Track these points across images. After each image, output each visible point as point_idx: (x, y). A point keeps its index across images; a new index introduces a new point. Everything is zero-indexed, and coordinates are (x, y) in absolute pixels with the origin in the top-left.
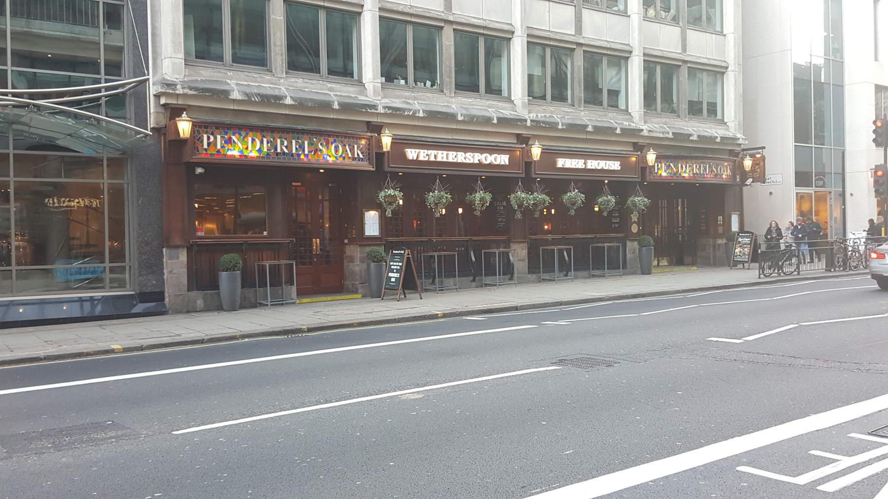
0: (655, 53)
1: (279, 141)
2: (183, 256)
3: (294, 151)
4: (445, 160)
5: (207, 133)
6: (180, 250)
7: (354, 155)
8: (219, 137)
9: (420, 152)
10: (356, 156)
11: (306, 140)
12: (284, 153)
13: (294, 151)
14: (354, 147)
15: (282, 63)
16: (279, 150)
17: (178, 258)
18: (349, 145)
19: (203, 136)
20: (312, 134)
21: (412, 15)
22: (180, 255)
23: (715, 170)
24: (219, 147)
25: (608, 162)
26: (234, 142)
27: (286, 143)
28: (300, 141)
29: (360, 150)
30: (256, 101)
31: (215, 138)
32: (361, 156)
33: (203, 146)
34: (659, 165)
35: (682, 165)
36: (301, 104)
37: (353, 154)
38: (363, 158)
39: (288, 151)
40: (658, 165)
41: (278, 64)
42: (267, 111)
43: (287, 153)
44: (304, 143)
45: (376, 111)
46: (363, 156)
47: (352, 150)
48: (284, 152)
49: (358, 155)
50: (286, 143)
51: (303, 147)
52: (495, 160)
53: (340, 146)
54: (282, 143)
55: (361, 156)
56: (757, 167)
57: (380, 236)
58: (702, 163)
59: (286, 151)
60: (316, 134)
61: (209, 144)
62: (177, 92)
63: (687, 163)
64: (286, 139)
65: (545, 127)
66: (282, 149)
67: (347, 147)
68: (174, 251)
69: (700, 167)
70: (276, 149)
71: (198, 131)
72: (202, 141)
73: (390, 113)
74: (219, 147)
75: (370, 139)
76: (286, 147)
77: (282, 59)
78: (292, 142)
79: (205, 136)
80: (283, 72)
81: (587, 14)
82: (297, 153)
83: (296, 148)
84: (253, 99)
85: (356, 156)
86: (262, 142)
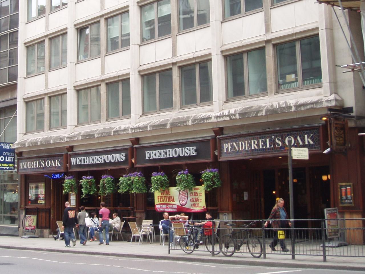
3: (261, 147)
11: (267, 138)
13: (261, 147)
14: (304, 137)
16: (253, 148)
18: (300, 136)
23: (43, 165)
25: (114, 155)
27: (256, 142)
29: (310, 138)
32: (312, 143)
35: (242, 143)
38: (313, 144)
44: (266, 141)
46: (313, 142)
47: (303, 140)
49: (308, 142)
51: (266, 144)
59: (256, 148)
60: (274, 133)
63: (228, 142)
64: (256, 140)
66: (254, 147)
67: (298, 138)
70: (251, 147)
76: (256, 145)
78: (259, 141)
82: (263, 148)
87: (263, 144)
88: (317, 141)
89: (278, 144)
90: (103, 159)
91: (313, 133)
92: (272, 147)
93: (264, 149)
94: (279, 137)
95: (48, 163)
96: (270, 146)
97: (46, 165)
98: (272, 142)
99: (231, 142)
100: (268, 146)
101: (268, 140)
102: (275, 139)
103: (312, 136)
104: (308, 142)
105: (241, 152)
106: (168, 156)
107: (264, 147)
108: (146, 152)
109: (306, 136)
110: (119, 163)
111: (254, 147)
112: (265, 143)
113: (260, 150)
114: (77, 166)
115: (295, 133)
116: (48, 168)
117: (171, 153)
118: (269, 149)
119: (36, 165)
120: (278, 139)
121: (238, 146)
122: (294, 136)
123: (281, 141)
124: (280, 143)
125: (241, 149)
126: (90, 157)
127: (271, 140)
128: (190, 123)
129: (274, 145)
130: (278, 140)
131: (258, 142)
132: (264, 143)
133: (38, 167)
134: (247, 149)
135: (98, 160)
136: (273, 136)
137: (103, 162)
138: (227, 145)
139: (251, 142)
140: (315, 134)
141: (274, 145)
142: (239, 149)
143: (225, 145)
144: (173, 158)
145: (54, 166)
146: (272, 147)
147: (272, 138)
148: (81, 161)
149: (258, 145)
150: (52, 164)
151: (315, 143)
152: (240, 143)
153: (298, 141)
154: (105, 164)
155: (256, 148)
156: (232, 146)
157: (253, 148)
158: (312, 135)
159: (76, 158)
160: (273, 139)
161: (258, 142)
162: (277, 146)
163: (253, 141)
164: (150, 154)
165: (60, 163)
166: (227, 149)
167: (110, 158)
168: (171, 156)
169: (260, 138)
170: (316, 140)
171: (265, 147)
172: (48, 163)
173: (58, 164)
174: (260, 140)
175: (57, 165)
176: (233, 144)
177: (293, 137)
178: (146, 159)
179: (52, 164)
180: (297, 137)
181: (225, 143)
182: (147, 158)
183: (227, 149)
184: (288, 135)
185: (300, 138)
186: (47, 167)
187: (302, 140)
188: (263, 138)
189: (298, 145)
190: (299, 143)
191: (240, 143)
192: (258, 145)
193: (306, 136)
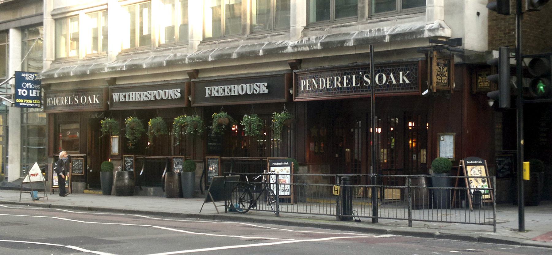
3: (345, 85)
7: (399, 81)
10: (401, 82)
11: (354, 75)
13: (345, 85)
14: (399, 74)
16: (335, 86)
20: (358, 69)
23: (77, 101)
25: (167, 91)
27: (340, 79)
28: (349, 76)
32: (407, 81)
35: (322, 80)
36: (361, 43)
38: (409, 83)
39: (341, 85)
42: (226, 65)
43: (340, 88)
48: (339, 87)
49: (403, 80)
50: (340, 79)
51: (351, 81)
55: (407, 81)
59: (340, 86)
63: (307, 79)
64: (340, 76)
66: (337, 85)
70: (334, 86)
76: (340, 82)
83: (347, 82)
87: (347, 81)
88: (414, 80)
89: (367, 83)
90: (153, 95)
91: (410, 70)
92: (359, 85)
94: (367, 73)
95: (83, 99)
96: (356, 84)
98: (360, 80)
100: (354, 85)
101: (354, 77)
102: (363, 75)
103: (409, 73)
104: (403, 80)
105: (321, 90)
106: (233, 94)
107: (349, 86)
108: (207, 88)
109: (401, 73)
111: (337, 85)
112: (350, 81)
115: (388, 70)
116: (83, 105)
117: (237, 90)
118: (354, 88)
119: (68, 102)
120: (366, 77)
121: (318, 84)
122: (387, 73)
123: (370, 79)
125: (321, 88)
126: (137, 93)
127: (358, 77)
129: (362, 84)
130: (367, 77)
131: (341, 80)
132: (349, 81)
134: (328, 87)
135: (146, 96)
136: (361, 71)
137: (153, 99)
139: (334, 79)
140: (412, 70)
141: (362, 84)
143: (302, 81)
145: (91, 102)
146: (359, 85)
147: (359, 75)
148: (125, 97)
150: (88, 101)
151: (412, 83)
152: (321, 79)
153: (391, 79)
155: (340, 86)
156: (311, 83)
158: (408, 72)
159: (118, 94)
160: (360, 76)
161: (342, 79)
162: (364, 85)
163: (335, 78)
164: (211, 91)
166: (305, 87)
167: (162, 94)
168: (236, 94)
169: (345, 74)
170: (413, 78)
171: (351, 86)
172: (83, 99)
173: (96, 100)
174: (345, 77)
175: (94, 102)
176: (312, 81)
177: (385, 74)
178: (206, 96)
179: (89, 100)
180: (390, 74)
181: (302, 79)
182: (207, 95)
183: (305, 87)
185: (394, 76)
186: (82, 104)
187: (395, 78)
188: (348, 75)
189: (391, 84)
190: (392, 82)
191: (321, 79)
193: (401, 73)
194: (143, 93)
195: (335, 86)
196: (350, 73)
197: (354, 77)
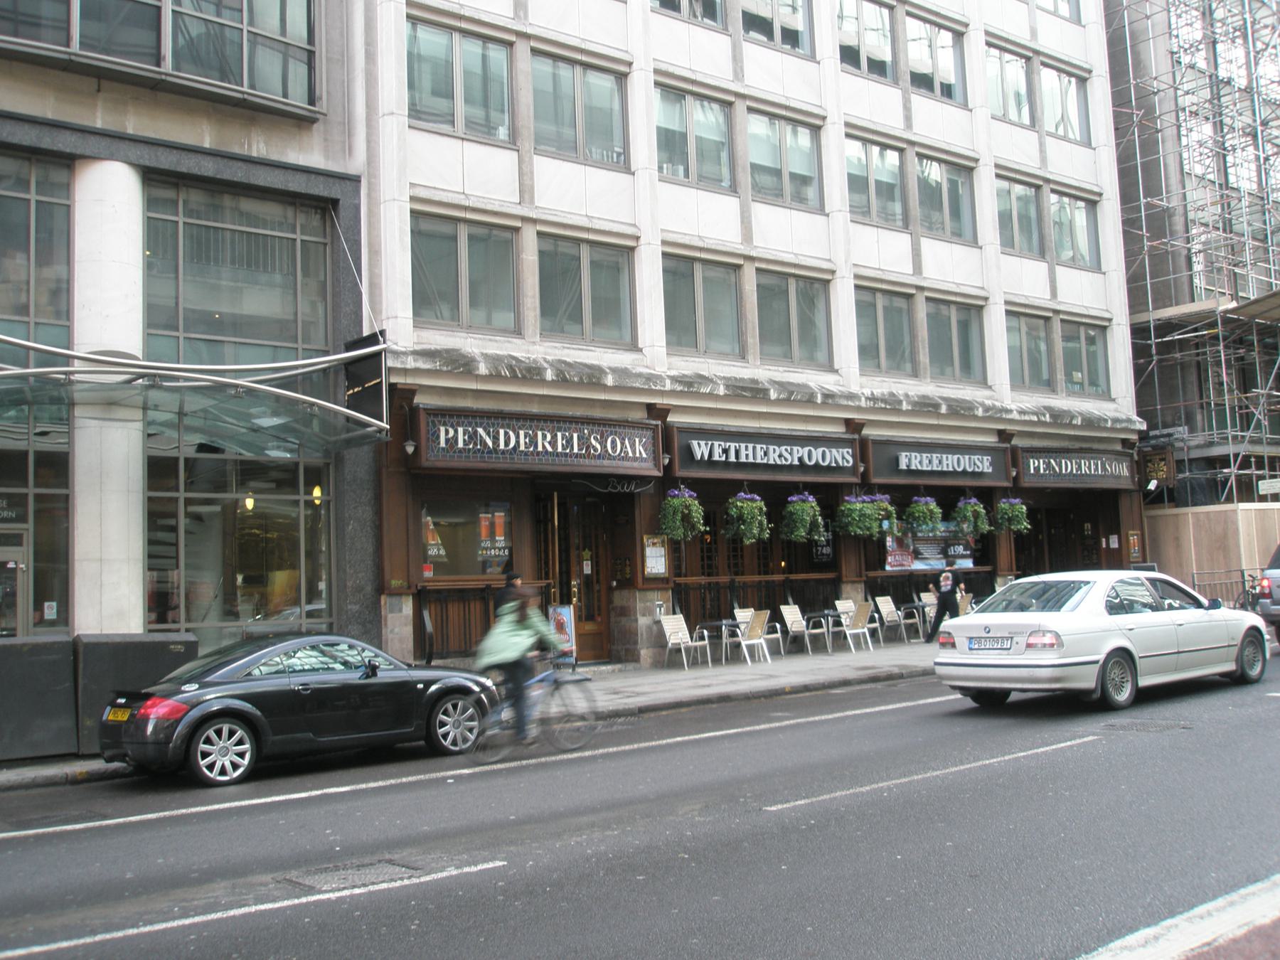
0: (1017, 300)
1: (540, 434)
2: (408, 607)
3: (560, 449)
4: (751, 460)
5: (445, 424)
6: (404, 598)
8: (460, 430)
9: (712, 445)
10: (638, 455)
12: (547, 452)
13: (560, 449)
15: (535, 321)
16: (540, 448)
17: (401, 610)
18: (629, 439)
19: (439, 429)
20: (583, 423)
21: (701, 249)
22: (404, 606)
24: (461, 444)
26: (481, 436)
27: (549, 437)
28: (567, 434)
30: (507, 376)
31: (456, 431)
32: (644, 455)
33: (439, 443)
34: (1036, 462)
37: (634, 452)
39: (553, 448)
40: (1034, 463)
41: (530, 323)
45: (662, 388)
47: (633, 446)
49: (640, 453)
52: (824, 458)
53: (617, 439)
54: (544, 437)
56: (1163, 463)
57: (667, 575)
58: (1092, 458)
59: (549, 449)
60: (588, 424)
61: (447, 441)
62: (408, 366)
64: (549, 431)
65: (885, 408)
66: (544, 446)
67: (627, 442)
68: (395, 600)
69: (1090, 464)
70: (536, 446)
71: (433, 422)
72: (438, 437)
73: (681, 391)
74: (461, 444)
75: (654, 429)
76: (550, 443)
77: (535, 316)
78: (556, 435)
79: (442, 429)
80: (536, 334)
81: (928, 245)
84: (503, 374)
85: (638, 455)
86: (518, 437)
87: (564, 442)
90: (796, 457)
93: (566, 455)
95: (613, 442)
97: (607, 451)
99: (1046, 457)
100: (576, 450)
101: (575, 436)
105: (1065, 475)
106: (945, 469)
108: (904, 454)
110: (838, 469)
111: (544, 446)
112: (569, 442)
113: (558, 455)
114: (710, 463)
117: (950, 462)
119: (1096, 469)
121: (496, 439)
123: (600, 443)
124: (598, 446)
126: (758, 446)
128: (980, 412)
129: (588, 448)
130: (596, 439)
132: (567, 442)
133: (576, 450)
134: (1074, 472)
135: (780, 456)
137: (796, 462)
138: (1036, 462)
139: (536, 435)
141: (588, 448)
142: (499, 446)
143: (1031, 461)
144: (954, 474)
145: (631, 454)
146: (584, 452)
147: (584, 433)
148: (726, 451)
149: (553, 443)
154: (802, 466)
156: (1048, 465)
157: (540, 448)
159: (710, 443)
161: (554, 437)
162: (592, 451)
164: (910, 460)
165: (645, 450)
166: (1037, 469)
167: (817, 455)
168: (951, 469)
169: (559, 429)
172: (613, 442)
174: (559, 434)
176: (1050, 462)
179: (626, 447)
181: (1033, 458)
183: (1037, 469)
184: (611, 434)
188: (565, 430)
192: (553, 443)
194: (774, 450)
195: (1083, 472)
196: (569, 429)
197: (575, 436)
